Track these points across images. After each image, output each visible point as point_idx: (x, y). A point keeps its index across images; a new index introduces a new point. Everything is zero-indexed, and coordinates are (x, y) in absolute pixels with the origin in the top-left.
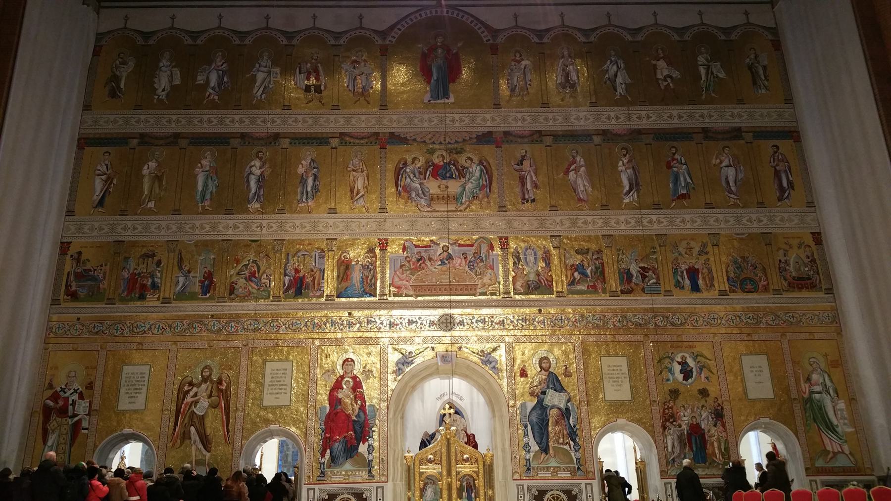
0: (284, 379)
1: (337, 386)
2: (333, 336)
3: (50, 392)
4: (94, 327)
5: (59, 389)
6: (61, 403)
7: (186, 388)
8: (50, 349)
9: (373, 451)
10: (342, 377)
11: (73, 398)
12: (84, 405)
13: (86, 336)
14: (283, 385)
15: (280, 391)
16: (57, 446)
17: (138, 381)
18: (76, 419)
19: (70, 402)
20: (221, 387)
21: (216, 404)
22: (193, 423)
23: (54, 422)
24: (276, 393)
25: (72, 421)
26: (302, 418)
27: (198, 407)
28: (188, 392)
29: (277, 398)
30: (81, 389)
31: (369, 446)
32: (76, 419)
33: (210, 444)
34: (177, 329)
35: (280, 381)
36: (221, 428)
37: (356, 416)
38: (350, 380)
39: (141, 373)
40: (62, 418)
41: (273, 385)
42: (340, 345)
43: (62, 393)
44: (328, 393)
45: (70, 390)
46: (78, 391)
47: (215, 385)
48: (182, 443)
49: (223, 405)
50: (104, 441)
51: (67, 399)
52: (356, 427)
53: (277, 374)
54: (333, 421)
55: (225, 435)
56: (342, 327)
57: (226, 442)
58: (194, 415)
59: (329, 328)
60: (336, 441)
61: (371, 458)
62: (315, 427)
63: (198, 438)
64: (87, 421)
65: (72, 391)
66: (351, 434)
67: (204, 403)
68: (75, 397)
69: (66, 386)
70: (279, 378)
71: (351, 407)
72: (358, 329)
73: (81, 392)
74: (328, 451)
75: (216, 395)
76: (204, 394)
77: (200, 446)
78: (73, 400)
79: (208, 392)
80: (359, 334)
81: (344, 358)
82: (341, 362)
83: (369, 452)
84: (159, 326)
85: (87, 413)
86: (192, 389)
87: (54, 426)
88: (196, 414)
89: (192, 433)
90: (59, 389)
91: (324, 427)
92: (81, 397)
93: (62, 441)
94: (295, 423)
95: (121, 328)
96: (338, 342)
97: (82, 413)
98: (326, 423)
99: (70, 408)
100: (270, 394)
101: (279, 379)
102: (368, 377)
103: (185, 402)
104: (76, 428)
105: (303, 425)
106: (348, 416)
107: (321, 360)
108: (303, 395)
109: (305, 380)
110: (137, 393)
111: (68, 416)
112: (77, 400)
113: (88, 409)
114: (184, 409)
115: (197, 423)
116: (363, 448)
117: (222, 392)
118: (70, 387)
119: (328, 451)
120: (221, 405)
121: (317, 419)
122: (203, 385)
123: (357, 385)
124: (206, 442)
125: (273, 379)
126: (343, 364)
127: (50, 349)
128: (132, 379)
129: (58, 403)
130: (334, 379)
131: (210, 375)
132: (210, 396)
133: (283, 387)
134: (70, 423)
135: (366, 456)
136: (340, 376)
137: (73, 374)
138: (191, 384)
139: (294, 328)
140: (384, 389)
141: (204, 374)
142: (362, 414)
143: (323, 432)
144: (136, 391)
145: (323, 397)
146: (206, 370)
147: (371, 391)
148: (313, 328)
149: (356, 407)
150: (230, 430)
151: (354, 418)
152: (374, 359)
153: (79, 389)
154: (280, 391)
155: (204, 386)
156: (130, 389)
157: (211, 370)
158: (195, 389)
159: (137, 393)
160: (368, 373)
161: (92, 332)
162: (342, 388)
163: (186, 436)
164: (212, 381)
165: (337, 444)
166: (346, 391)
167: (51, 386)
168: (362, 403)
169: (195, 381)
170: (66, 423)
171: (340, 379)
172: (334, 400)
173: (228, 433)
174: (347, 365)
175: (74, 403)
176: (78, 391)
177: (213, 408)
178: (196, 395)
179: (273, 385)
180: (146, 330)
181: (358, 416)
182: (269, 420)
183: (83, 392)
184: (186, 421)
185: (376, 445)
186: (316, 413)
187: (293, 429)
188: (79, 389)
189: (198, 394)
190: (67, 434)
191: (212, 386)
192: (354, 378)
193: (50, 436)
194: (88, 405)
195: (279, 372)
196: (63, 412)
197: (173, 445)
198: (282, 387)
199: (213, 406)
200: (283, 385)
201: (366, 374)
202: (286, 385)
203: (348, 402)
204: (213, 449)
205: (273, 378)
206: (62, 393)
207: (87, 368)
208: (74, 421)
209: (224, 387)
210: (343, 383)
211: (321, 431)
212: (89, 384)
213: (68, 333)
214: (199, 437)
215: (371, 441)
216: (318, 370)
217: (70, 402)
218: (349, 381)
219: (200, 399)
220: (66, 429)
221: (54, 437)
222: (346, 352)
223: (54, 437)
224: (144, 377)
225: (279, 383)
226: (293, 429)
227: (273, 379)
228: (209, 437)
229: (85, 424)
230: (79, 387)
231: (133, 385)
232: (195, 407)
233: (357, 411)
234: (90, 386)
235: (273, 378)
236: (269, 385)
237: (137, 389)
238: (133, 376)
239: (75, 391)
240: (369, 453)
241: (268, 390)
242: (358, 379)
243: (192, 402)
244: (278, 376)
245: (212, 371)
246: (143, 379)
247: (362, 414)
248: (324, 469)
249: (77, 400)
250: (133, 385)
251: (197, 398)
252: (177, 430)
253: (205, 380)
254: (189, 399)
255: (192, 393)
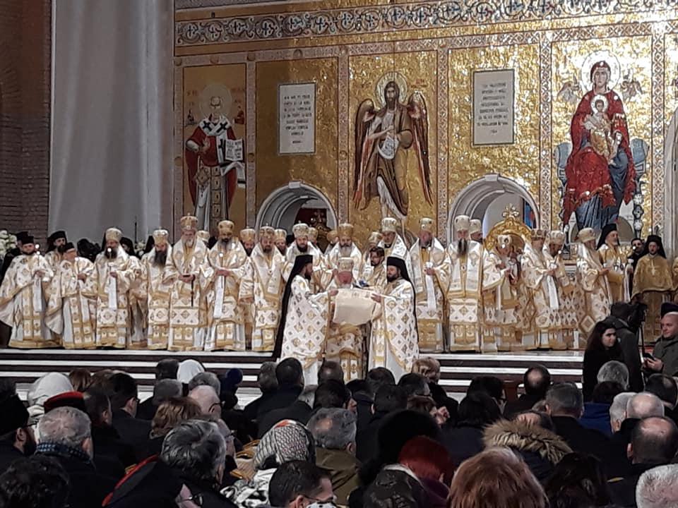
0: (503, 100)
1: (583, 111)
2: (575, 23)
3: (190, 131)
4: (235, 27)
5: (202, 124)
6: (207, 145)
7: (366, 118)
8: (184, 65)
9: (641, 215)
10: (591, 94)
11: (221, 137)
12: (236, 147)
13: (226, 41)
14: (500, 110)
15: (496, 120)
16: (211, 207)
17: (301, 108)
18: (229, 168)
19: (218, 143)
20: (413, 116)
21: (409, 141)
22: (380, 172)
23: (203, 171)
24: (491, 124)
25: (224, 171)
26: (532, 162)
27: (384, 147)
28: (369, 124)
29: (494, 132)
30: (229, 124)
31: (636, 206)
32: (229, 168)
33: (407, 203)
34: (345, 23)
35: (495, 104)
36: (418, 179)
37: (614, 159)
38: (604, 99)
39: (304, 96)
40: (211, 166)
41: (486, 111)
42: (586, 40)
43: (206, 130)
44: (569, 122)
45: (215, 124)
46: (227, 127)
47: (405, 112)
48: (368, 201)
49: (418, 144)
50: (266, 201)
51: (213, 139)
52: (614, 177)
53: (491, 92)
54: (578, 166)
55: (424, 190)
56: (588, 7)
57: (427, 199)
58: (381, 160)
59: (567, 10)
60: (584, 199)
61: (638, 225)
62: (553, 176)
63: (388, 195)
64: (243, 171)
65: (219, 126)
66: (608, 189)
67: (392, 142)
68: (223, 135)
69: (210, 119)
70: (496, 98)
71: (607, 145)
72: (615, 9)
73: (230, 128)
74: (573, 215)
75: (408, 127)
76: (391, 127)
77: (393, 206)
78: (221, 140)
79: (397, 124)
80: (618, 18)
81: (594, 63)
82: (587, 69)
83: (635, 216)
84: (321, 20)
85: (241, 159)
86: (374, 118)
87: (202, 178)
88: (383, 158)
89: (379, 185)
90: (202, 124)
91: (565, 178)
92: (231, 135)
93: (214, 198)
94: (523, 169)
95: (270, 26)
96: (583, 33)
97: (235, 159)
98: (568, 170)
99: (220, 151)
100: (483, 124)
101: (493, 101)
102: (632, 93)
103: (366, 140)
104: (230, 178)
105: (534, 174)
106: (602, 159)
107: (557, 66)
108: (531, 125)
109: (533, 101)
110: (302, 127)
111: (218, 164)
112: (227, 140)
113: (241, 152)
114: (367, 150)
115: (385, 170)
116: (625, 211)
117: (415, 124)
118: (216, 121)
119: (573, 215)
120: (416, 143)
121: (554, 165)
122: (388, 114)
123: (615, 107)
124: (400, 200)
125: (487, 101)
126: (592, 72)
127: (184, 65)
128: (292, 106)
129: (203, 145)
130: (578, 97)
131: (397, 97)
132: (399, 131)
133: (502, 114)
134: (222, 174)
135: (631, 223)
136: (588, 93)
137: (216, 100)
138: (371, 111)
139: (513, 13)
140: (658, 113)
141: (388, 95)
142: (623, 156)
143: (564, 184)
144: (300, 124)
145: (562, 131)
146: (391, 89)
147: (637, 112)
148: (543, 10)
149: (615, 145)
150: (431, 182)
151: (612, 162)
152: (645, 62)
153: (226, 123)
154: (496, 120)
155: (389, 114)
156: (293, 122)
157: (396, 88)
158: (378, 119)
159: (302, 127)
160: (631, 86)
161: (233, 34)
162: (591, 113)
163: (372, 192)
164: (399, 106)
165: (586, 204)
166: (598, 118)
167: (192, 121)
168: (623, 138)
169: (377, 108)
170: (217, 174)
171: (587, 98)
172: (578, 133)
173: (428, 186)
174: (598, 73)
175: (223, 146)
176: (227, 127)
177: (406, 148)
178: (379, 129)
179: (486, 111)
180: (303, 27)
181: (617, 158)
182: (483, 166)
183: (233, 127)
184: (370, 170)
185: (647, 204)
186: (553, 155)
187: (520, 181)
188: (226, 123)
189: (383, 127)
190: (219, 189)
191: (401, 114)
192: (610, 95)
193: (200, 194)
194: (241, 146)
195: (494, 89)
196: (211, 158)
197: (356, 206)
198: (500, 113)
199: (405, 145)
200: (500, 110)
201: (628, 87)
202: (506, 110)
203: (600, 136)
204: (409, 210)
205: (485, 98)
206: (206, 130)
207: (233, 90)
208: (226, 172)
209: (417, 116)
210: (593, 104)
211: (561, 184)
212: (239, 116)
213: (203, 38)
214: (390, 192)
215: (638, 199)
216: (554, 83)
217: (218, 143)
218: (602, 102)
219: (386, 133)
220: (219, 183)
221: (204, 193)
222: (595, 51)
223: (204, 193)
224: (308, 103)
225: (495, 108)
226: (520, 181)
227: (487, 101)
228: (403, 193)
229: (240, 175)
230: (227, 120)
231: (296, 115)
232: (381, 147)
233: (616, 151)
234: (240, 119)
235: (485, 98)
236: (482, 111)
237: (301, 121)
238: (294, 100)
239: (223, 126)
240: (636, 219)
241: (480, 118)
242: (616, 98)
243: (376, 140)
244: (492, 95)
245: (399, 90)
246: (308, 106)
247: (623, 156)
248: (568, 242)
249: (227, 140)
250: (296, 115)
251: (382, 133)
252: (359, 182)
253: (391, 103)
254: (371, 135)
255: (374, 127)
